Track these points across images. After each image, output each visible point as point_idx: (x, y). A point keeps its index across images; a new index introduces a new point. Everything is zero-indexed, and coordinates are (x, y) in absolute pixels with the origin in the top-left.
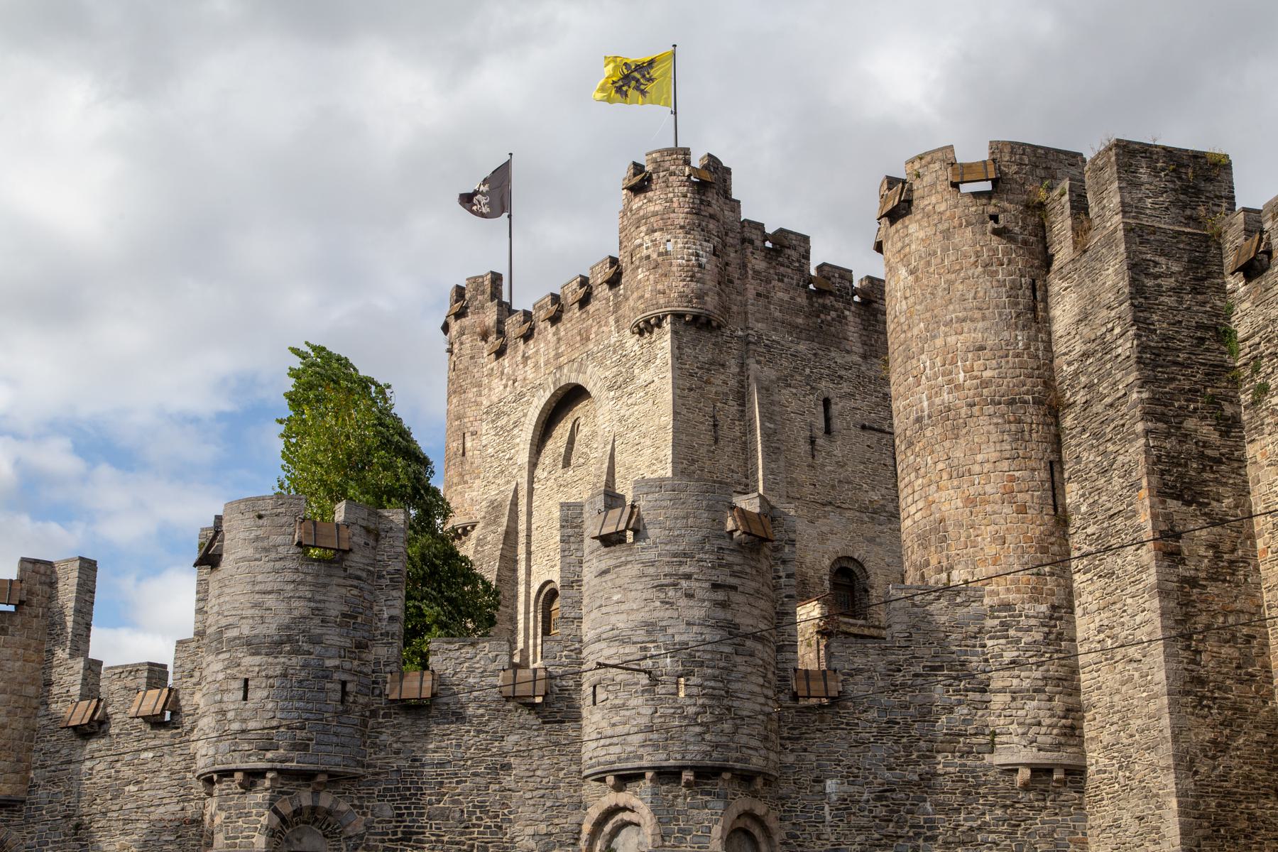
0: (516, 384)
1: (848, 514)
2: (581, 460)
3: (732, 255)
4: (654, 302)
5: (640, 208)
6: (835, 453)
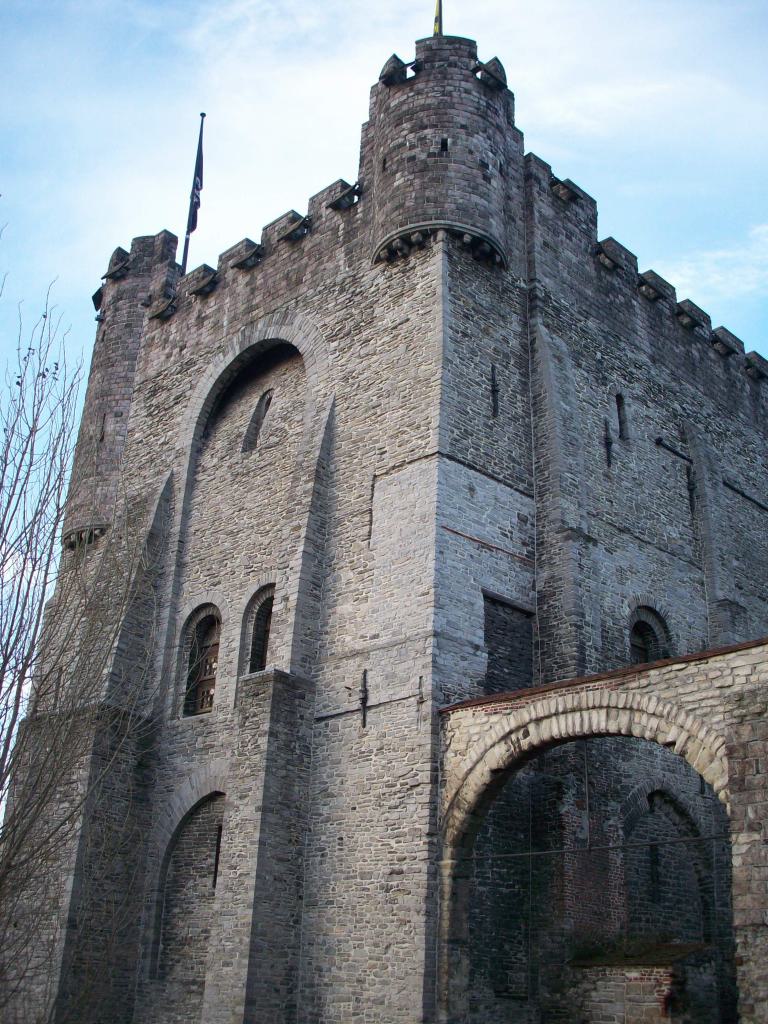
0: (184, 352)
1: (649, 549)
3: (515, 190)
4: (420, 211)
5: (402, 103)
6: (631, 465)
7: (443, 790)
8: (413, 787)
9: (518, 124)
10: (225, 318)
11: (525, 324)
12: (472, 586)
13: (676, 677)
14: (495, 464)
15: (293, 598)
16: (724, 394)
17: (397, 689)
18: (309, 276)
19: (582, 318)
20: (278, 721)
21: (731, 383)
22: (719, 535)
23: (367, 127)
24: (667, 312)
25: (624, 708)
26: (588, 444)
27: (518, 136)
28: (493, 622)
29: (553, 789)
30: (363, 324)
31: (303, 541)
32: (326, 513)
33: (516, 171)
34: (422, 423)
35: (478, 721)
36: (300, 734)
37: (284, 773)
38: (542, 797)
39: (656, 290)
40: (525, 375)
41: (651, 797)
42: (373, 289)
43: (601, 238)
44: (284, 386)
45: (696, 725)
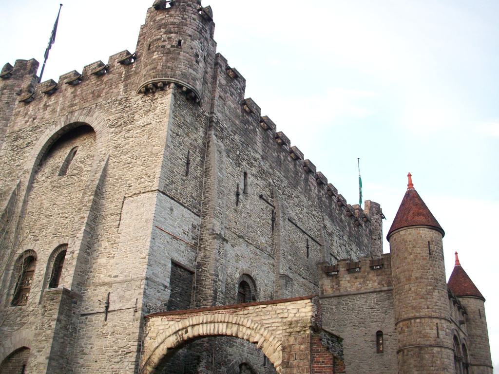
1: (251, 247)
2: (75, 172)
3: (209, 69)
4: (164, 72)
5: (162, 19)
6: (248, 206)
7: (143, 356)
8: (127, 353)
9: (215, 39)
10: (59, 107)
11: (206, 133)
12: (167, 257)
13: (261, 311)
14: (184, 199)
15: (77, 253)
16: (293, 177)
17: (124, 304)
18: (104, 94)
19: (233, 134)
21: (296, 173)
22: (284, 243)
23: (143, 27)
24: (272, 136)
25: (235, 324)
26: (228, 194)
27: (214, 44)
28: (175, 275)
29: (195, 359)
31: (85, 225)
33: (211, 60)
34: (152, 174)
35: (163, 323)
36: (72, 321)
37: (62, 340)
38: (190, 362)
39: (267, 126)
40: (203, 158)
41: (240, 366)
42: (135, 106)
43: (246, 97)
44: (84, 146)
45: (269, 334)
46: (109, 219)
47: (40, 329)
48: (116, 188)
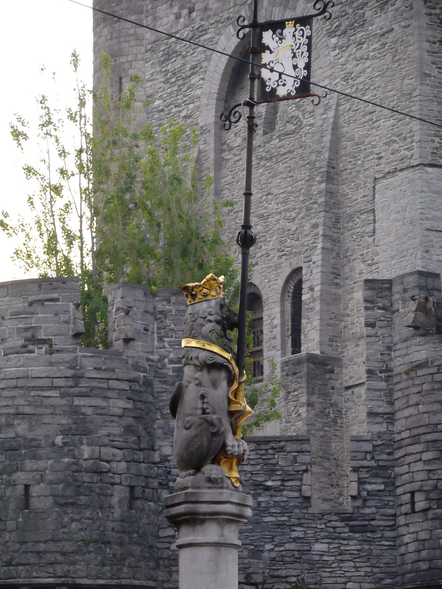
0: (194, 14)
2: (290, 127)
20: (313, 394)
30: (356, 25)
31: (320, 239)
32: (339, 208)
34: (408, 135)
36: (332, 401)
37: (322, 433)
46: (358, 220)
47: (287, 422)
48: (359, 162)
